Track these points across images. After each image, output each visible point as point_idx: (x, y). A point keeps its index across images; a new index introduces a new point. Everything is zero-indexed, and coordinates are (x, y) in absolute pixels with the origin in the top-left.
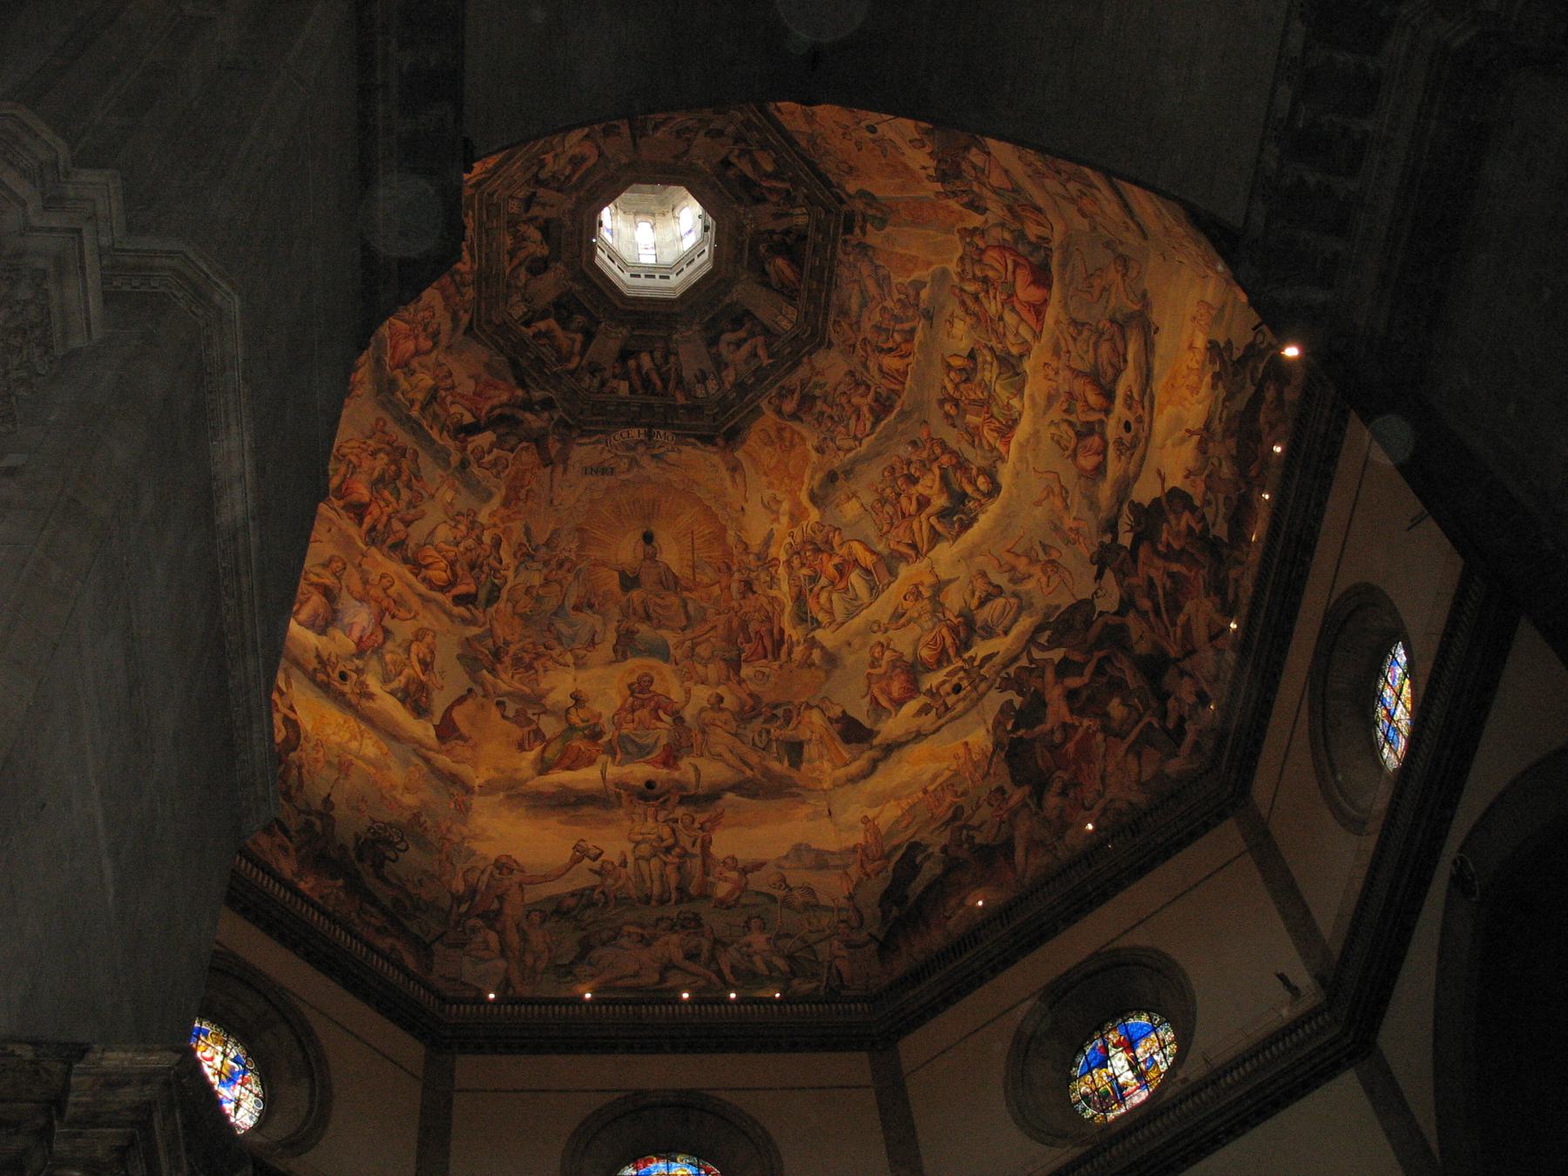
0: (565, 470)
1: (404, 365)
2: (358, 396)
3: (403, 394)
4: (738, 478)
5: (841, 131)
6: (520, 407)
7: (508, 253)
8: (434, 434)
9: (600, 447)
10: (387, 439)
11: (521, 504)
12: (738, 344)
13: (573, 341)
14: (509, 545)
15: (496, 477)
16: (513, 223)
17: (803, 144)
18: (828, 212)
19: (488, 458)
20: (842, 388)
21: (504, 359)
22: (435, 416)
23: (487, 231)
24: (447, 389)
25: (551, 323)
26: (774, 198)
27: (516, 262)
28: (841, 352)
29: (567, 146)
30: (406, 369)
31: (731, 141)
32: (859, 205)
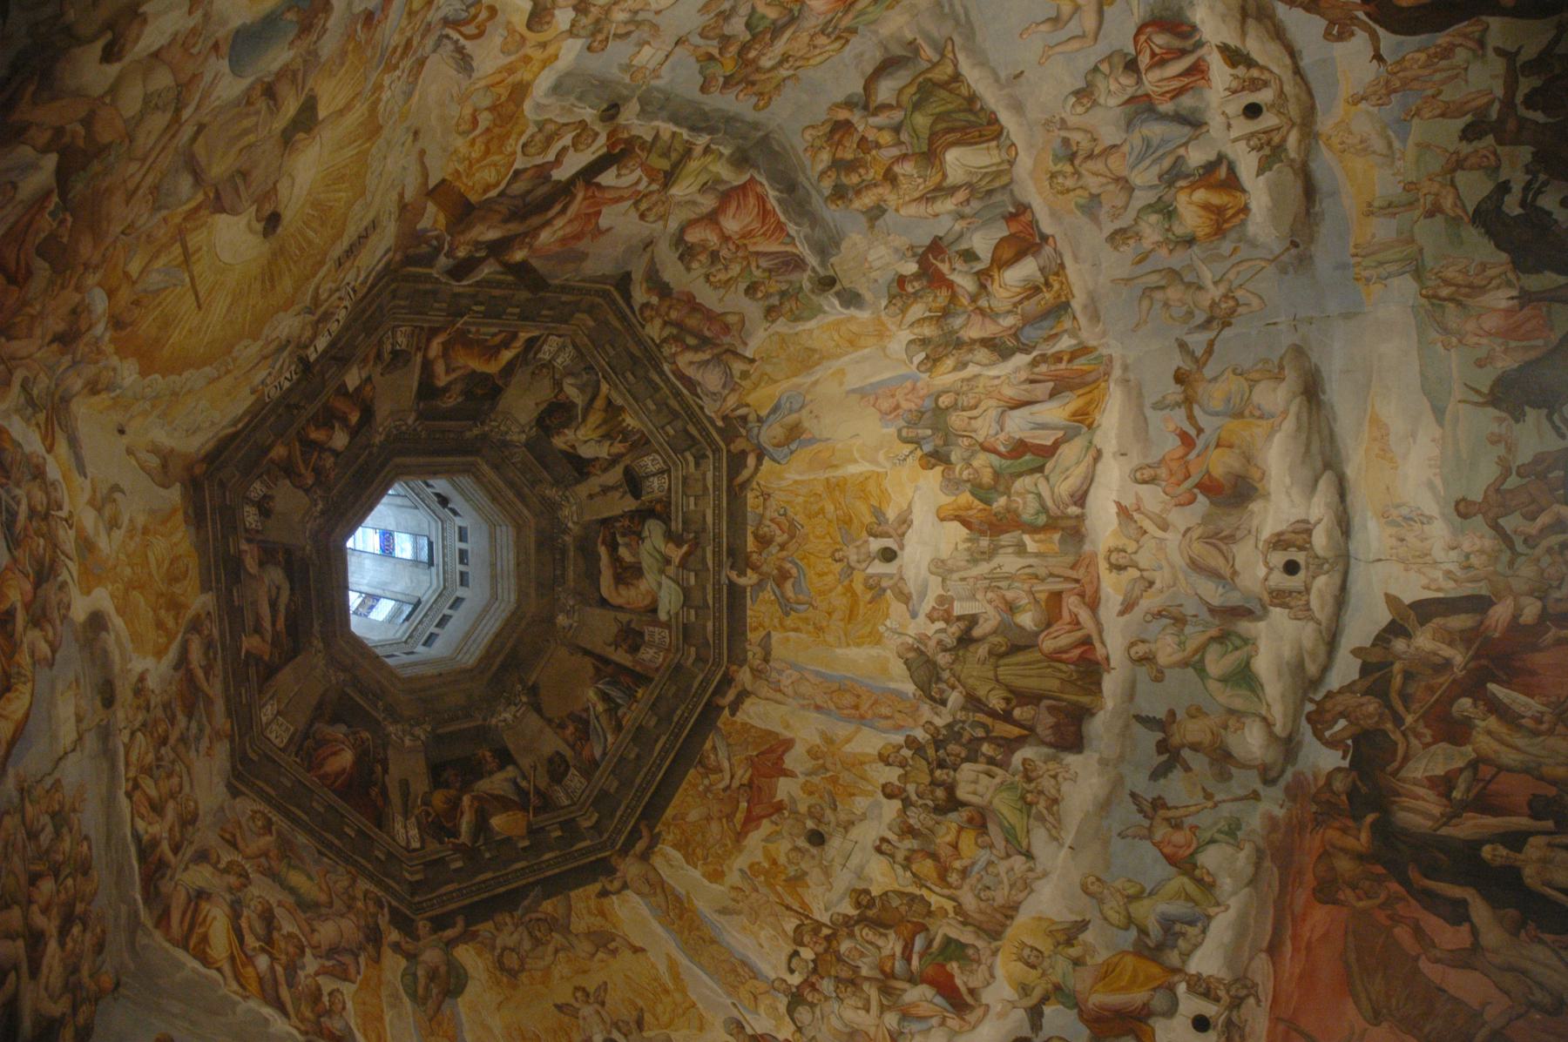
0: (401, 195)
1: (728, 196)
2: (813, 127)
3: (721, 155)
4: (154, 462)
5: (591, 990)
6: (516, 236)
7: (622, 409)
8: (667, 128)
9: (363, 275)
10: (755, 88)
11: (487, 102)
12: (273, 605)
13: (447, 372)
14: (509, 23)
15: (551, 120)
16: (641, 444)
17: (547, 906)
18: (415, 888)
19: (567, 140)
20: (187, 789)
21: (557, 282)
22: (665, 154)
23: (676, 416)
24: (645, 196)
25: (493, 368)
26: (439, 799)
27: (600, 403)
28: (222, 809)
29: (664, 580)
30: (722, 188)
31: (543, 785)
32: (431, 956)
